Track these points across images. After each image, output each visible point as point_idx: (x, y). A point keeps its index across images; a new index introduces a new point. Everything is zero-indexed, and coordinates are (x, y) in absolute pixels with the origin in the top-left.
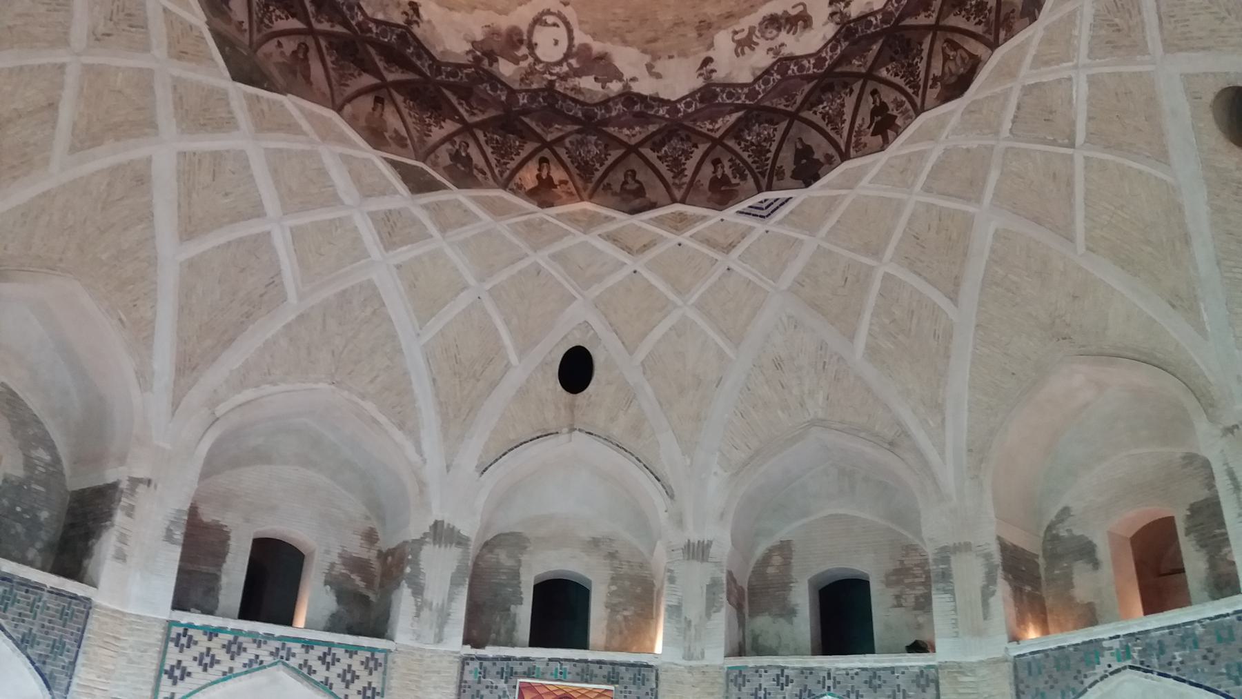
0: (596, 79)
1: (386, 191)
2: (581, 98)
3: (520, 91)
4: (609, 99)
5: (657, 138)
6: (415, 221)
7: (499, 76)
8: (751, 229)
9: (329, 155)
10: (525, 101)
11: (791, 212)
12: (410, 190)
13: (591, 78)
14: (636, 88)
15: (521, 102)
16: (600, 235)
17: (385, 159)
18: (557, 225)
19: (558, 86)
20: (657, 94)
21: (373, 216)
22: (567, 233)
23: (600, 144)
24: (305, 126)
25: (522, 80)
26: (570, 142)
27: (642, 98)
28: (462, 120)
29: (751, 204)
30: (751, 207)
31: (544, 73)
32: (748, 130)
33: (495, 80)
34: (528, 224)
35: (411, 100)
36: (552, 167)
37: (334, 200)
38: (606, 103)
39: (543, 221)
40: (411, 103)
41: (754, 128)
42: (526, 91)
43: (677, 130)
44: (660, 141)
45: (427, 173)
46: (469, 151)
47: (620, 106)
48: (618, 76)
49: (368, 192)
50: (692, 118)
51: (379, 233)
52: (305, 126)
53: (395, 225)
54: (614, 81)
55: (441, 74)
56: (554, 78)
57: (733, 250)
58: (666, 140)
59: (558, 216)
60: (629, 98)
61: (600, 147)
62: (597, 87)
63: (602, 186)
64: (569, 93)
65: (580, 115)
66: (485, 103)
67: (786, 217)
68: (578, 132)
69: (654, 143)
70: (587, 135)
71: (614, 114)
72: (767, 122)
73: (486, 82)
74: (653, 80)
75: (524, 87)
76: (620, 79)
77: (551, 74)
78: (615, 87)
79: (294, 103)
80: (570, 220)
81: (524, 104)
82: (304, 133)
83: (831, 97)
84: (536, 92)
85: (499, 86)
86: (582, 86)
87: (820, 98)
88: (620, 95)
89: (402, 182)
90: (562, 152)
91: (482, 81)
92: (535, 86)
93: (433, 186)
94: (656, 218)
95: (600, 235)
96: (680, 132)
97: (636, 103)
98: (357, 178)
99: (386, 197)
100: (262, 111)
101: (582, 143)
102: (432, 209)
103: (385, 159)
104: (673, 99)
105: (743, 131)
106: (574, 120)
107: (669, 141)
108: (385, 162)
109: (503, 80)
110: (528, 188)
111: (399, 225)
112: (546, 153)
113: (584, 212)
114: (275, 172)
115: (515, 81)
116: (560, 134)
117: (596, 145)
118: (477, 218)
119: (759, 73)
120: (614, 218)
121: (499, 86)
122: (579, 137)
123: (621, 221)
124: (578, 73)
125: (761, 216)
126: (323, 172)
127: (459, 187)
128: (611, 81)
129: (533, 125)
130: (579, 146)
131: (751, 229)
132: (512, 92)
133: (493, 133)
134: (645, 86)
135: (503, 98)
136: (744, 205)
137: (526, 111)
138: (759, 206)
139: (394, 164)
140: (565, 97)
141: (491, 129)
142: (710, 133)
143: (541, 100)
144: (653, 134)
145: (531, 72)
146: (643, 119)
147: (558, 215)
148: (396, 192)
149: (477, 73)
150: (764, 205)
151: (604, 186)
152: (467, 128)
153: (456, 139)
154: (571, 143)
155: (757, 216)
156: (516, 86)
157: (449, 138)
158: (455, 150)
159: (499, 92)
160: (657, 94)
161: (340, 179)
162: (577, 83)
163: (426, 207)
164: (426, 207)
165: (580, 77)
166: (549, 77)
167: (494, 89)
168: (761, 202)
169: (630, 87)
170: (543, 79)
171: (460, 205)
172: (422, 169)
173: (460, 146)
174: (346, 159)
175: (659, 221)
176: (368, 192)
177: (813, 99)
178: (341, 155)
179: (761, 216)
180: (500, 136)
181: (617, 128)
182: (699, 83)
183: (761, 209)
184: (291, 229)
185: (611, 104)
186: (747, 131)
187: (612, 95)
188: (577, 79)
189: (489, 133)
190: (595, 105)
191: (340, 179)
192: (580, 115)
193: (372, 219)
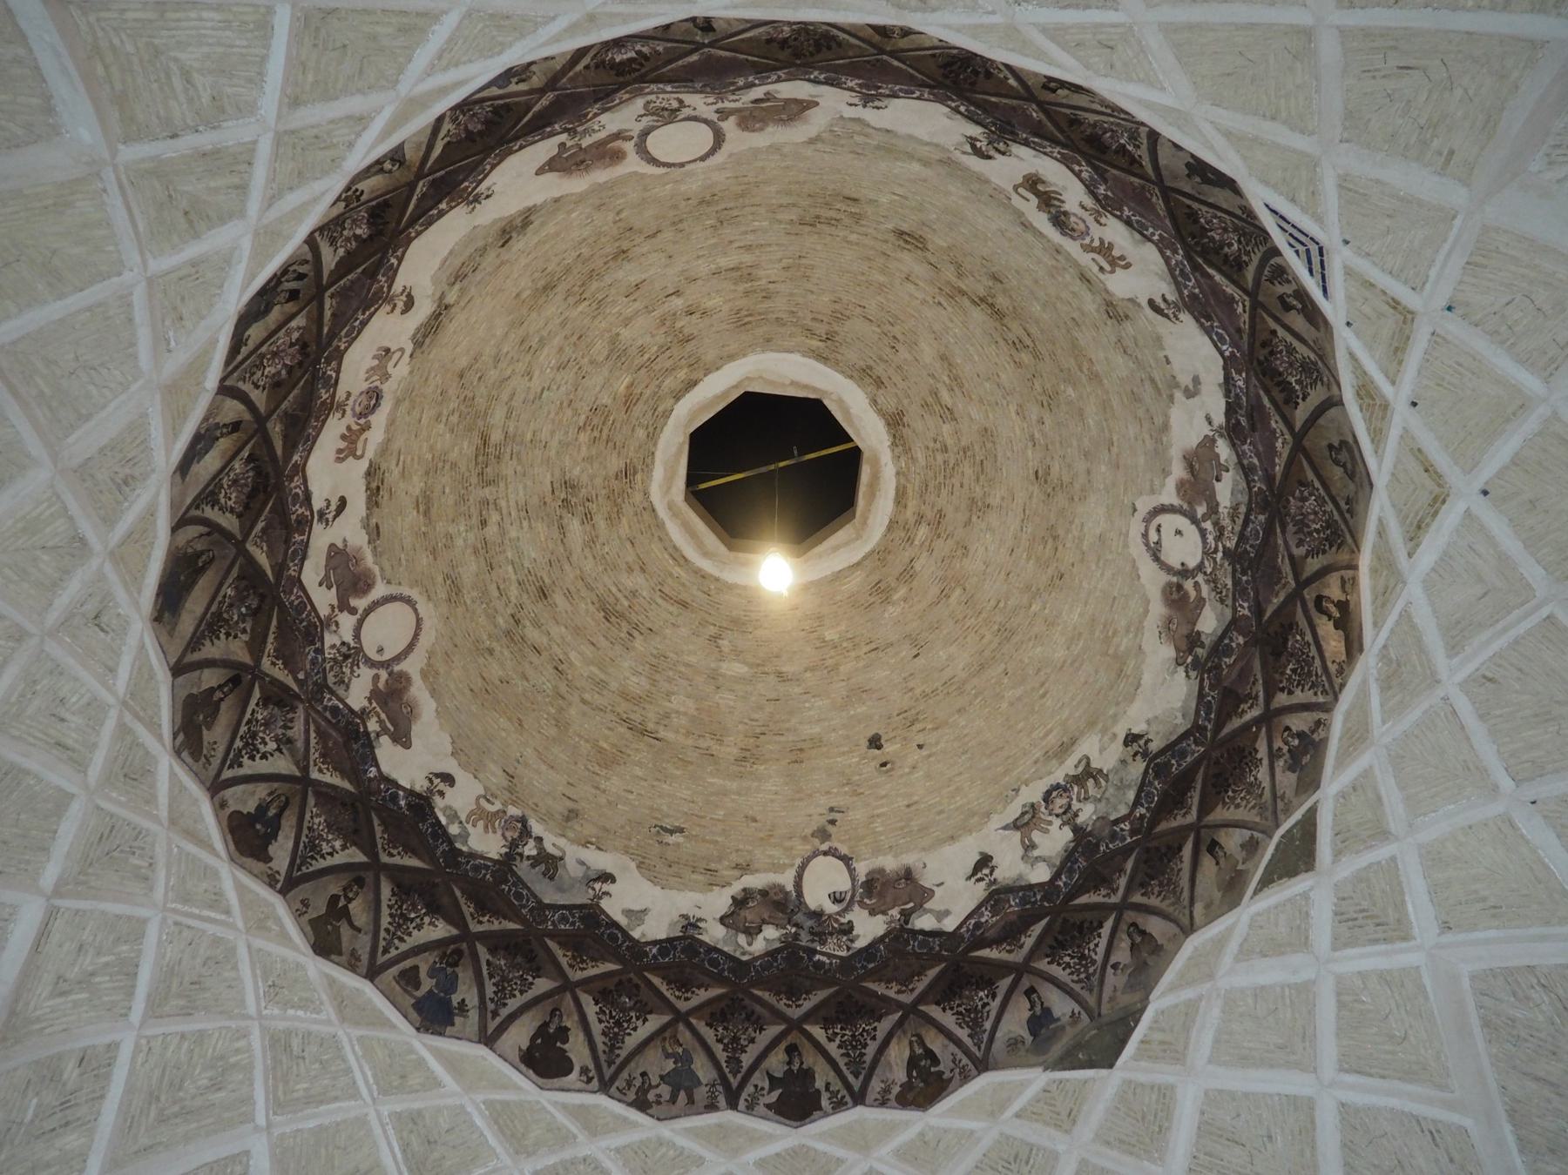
0: (1218, 480)
1: (1301, 909)
2: (1243, 509)
3: (1235, 610)
4: (1240, 463)
5: (1280, 397)
6: (1360, 878)
7: (1215, 638)
8: (1349, 272)
9: (1236, 976)
10: (1246, 605)
11: (1293, 200)
12: (1306, 871)
13: (1218, 486)
14: (1219, 419)
15: (1246, 612)
16: (1410, 555)
17: (1256, 893)
18: (1392, 631)
19: (1231, 544)
20: (1220, 385)
21: (1338, 943)
22: (1406, 616)
23: (1302, 492)
24: (1188, 994)
25: (1222, 601)
26: (1298, 546)
27: (1230, 410)
28: (1257, 721)
29: (1306, 272)
30: (1311, 271)
31: (1214, 559)
32: (1222, 248)
33: (1220, 647)
34: (1386, 685)
35: (1227, 792)
36: (1326, 593)
37: (1304, 993)
38: (1247, 471)
39: (1384, 655)
40: (1230, 793)
41: (1217, 237)
42: (1234, 600)
43: (1260, 363)
44: (1281, 391)
45: (1288, 831)
46: (1294, 729)
47: (1246, 447)
48: (1209, 442)
49: (1300, 940)
50: (1237, 337)
51: (1376, 941)
52: (1188, 994)
53: (1364, 911)
54: (1217, 450)
55: (1206, 728)
56: (1221, 548)
57: (1404, 302)
58: (1281, 379)
59: (1377, 625)
60: (1233, 432)
61: (1306, 493)
62: (1228, 478)
63: (1348, 516)
64: (1238, 528)
65: (1262, 518)
66: (1244, 674)
67: (1304, 210)
68: (1283, 532)
69: (1287, 402)
70: (1288, 514)
71: (1255, 461)
72: (1196, 221)
73: (1220, 659)
74: (1204, 388)
75: (1229, 602)
76: (1213, 441)
77: (1216, 551)
78: (1223, 450)
79: (1163, 994)
80: (1383, 605)
81: (1249, 608)
82: (1200, 998)
83: (1108, 135)
84: (1236, 582)
85: (1226, 641)
86: (1228, 505)
87: (1117, 152)
88: (1233, 445)
89: (1293, 880)
90: (1313, 565)
91: (1218, 667)
92: (1229, 582)
93: (1308, 826)
94: (1373, 441)
95: (1410, 555)
96: (1262, 358)
97: (1238, 422)
98: (1275, 949)
99: (1312, 913)
100: (1162, 1043)
101: (1302, 525)
102: (1346, 841)
103: (1256, 893)
104: (1221, 362)
105: (1226, 255)
106: (1269, 530)
107: (1280, 374)
108: (1257, 897)
109: (1219, 632)
110: (1344, 657)
111: (1365, 904)
112: (1309, 594)
113: (1374, 571)
114: (1245, 1060)
115: (1222, 614)
116: (1287, 561)
117: (1304, 499)
118: (1367, 773)
119: (1138, 236)
120: (1380, 520)
121: (1226, 641)
122: (1291, 528)
123: (1382, 508)
124: (1213, 509)
125: (1321, 254)
126: (1259, 992)
127: (1318, 787)
128: (1218, 456)
129: (1276, 601)
130: (1306, 530)
131: (1349, 272)
132: (1234, 624)
133: (1283, 673)
134: (1215, 404)
135: (1241, 640)
136: (1312, 286)
137: (1258, 610)
138: (1304, 256)
139: (1266, 882)
140: (1242, 537)
141: (1277, 676)
142: (1247, 309)
143: (1244, 578)
144: (1273, 401)
145: (1213, 580)
146: (1256, 412)
147: (1375, 624)
148: (1305, 896)
149: (1209, 671)
150: (1301, 249)
151: (1348, 511)
152: (1269, 717)
153: (1275, 747)
154: (1300, 543)
155: (1322, 262)
156: (1228, 613)
157: (1273, 756)
158: (1287, 755)
159: (1234, 645)
160: (1220, 385)
161: (1270, 973)
162: (1226, 511)
163: (1337, 854)
164: (1337, 854)
165: (1218, 504)
166: (1220, 555)
167: (1228, 651)
168: (1297, 252)
169: (1220, 427)
170: (1222, 566)
171: (1343, 795)
172: (1283, 837)
173: (1286, 743)
174: (1245, 953)
175: (1378, 436)
176: (1300, 940)
177: (1123, 162)
178: (1237, 960)
179: (1321, 254)
180: (1289, 662)
181: (1277, 460)
182: (1186, 317)
183: (1308, 251)
184: (1342, 1070)
185: (1245, 462)
186: (1226, 249)
187: (1234, 458)
188: (1220, 510)
189: (1281, 682)
190: (1250, 488)
191: (1270, 973)
192: (1262, 518)
193: (1346, 945)
